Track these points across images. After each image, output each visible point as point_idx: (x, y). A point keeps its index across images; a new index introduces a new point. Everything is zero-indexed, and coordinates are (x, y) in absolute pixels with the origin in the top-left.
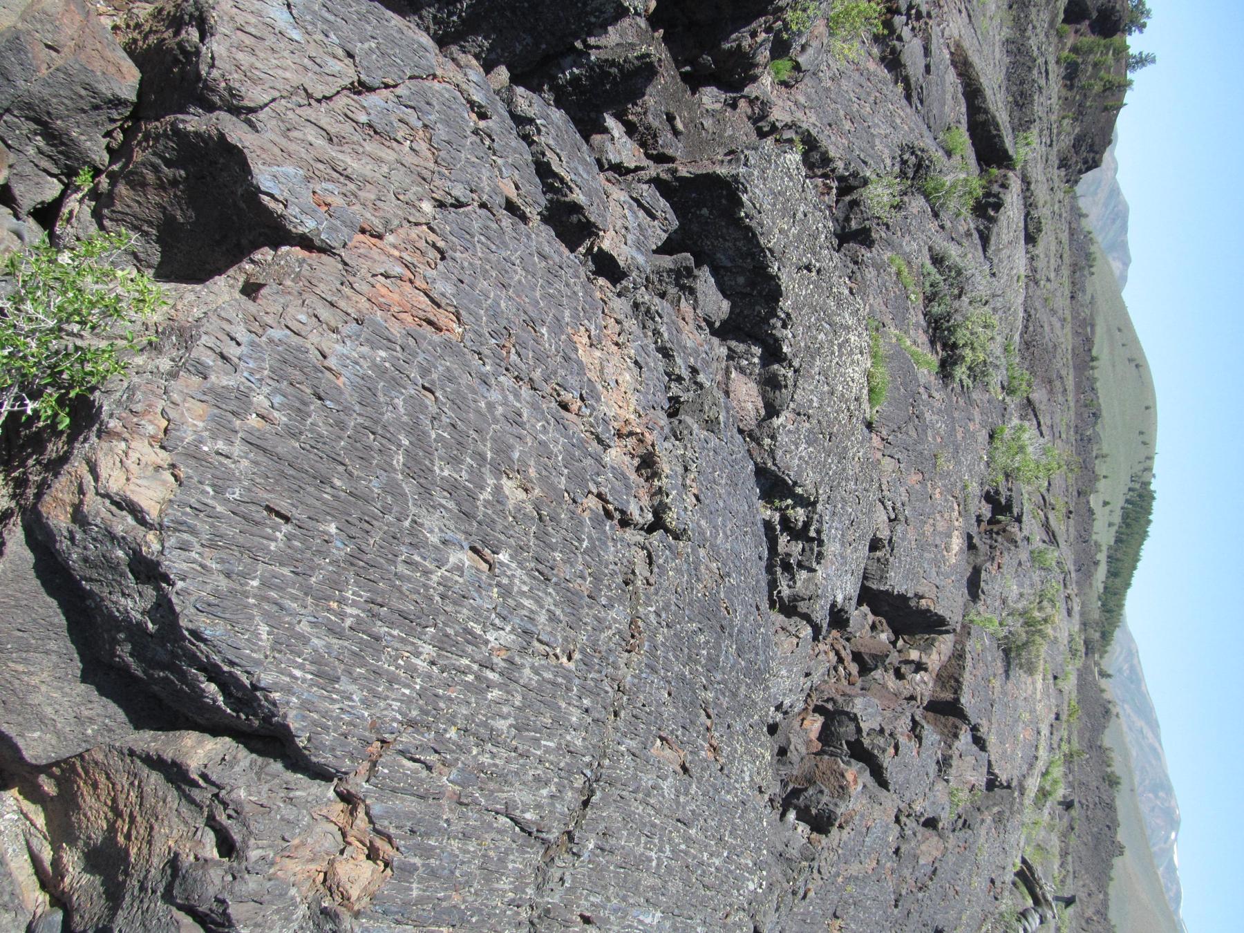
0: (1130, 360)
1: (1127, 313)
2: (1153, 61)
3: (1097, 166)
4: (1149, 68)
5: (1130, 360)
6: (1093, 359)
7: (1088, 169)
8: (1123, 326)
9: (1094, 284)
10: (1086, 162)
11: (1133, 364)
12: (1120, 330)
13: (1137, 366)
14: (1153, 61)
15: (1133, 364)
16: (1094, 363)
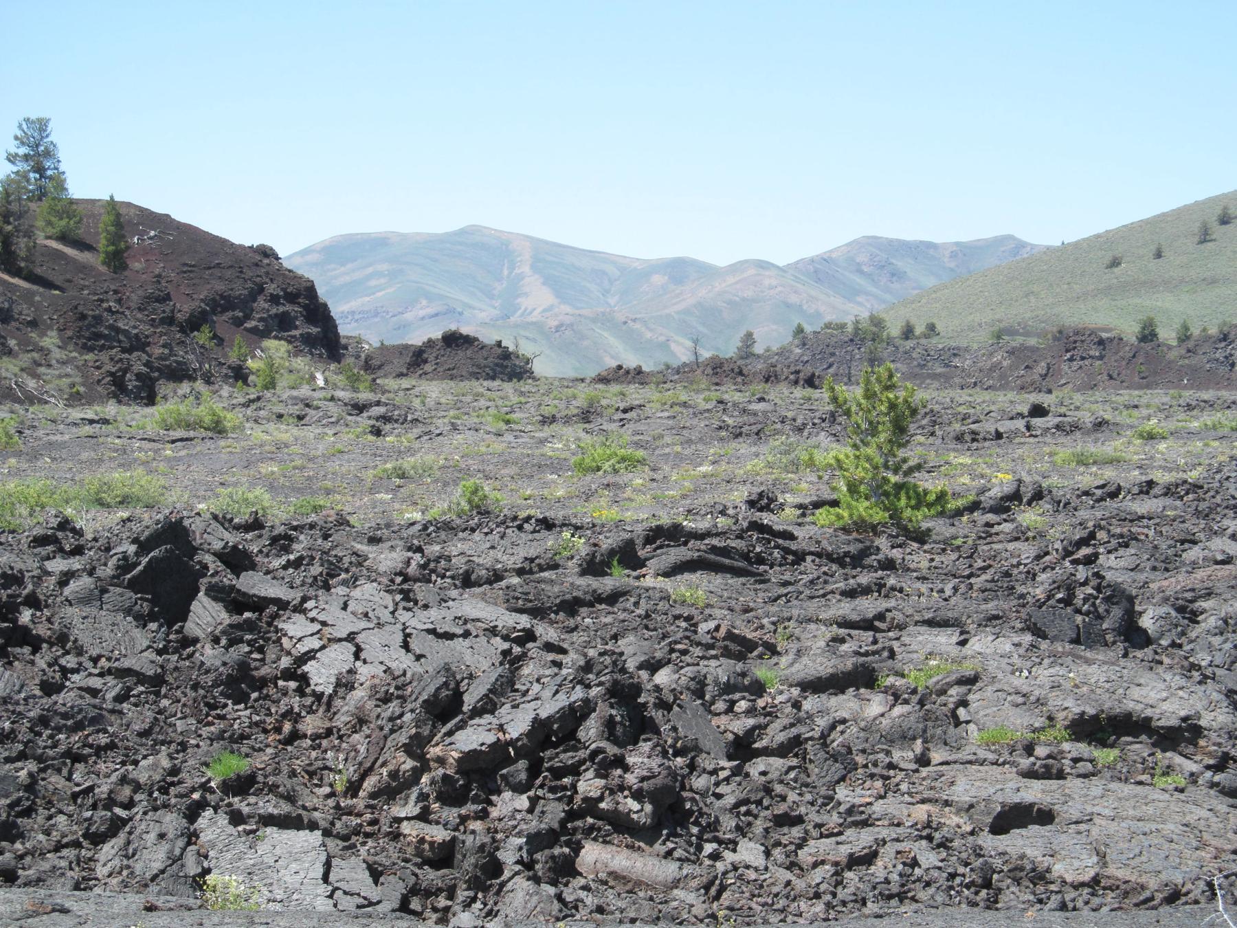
0: (1205, 237)
1: (1077, 245)
2: (41, 126)
3: (311, 290)
4: (56, 135)
5: (1205, 237)
6: (1148, 335)
7: (318, 313)
8: (1110, 255)
9: (965, 325)
10: (283, 324)
11: (1218, 231)
12: (1115, 263)
13: (1225, 220)
14: (41, 126)
15: (1218, 231)
16: (1168, 334)
